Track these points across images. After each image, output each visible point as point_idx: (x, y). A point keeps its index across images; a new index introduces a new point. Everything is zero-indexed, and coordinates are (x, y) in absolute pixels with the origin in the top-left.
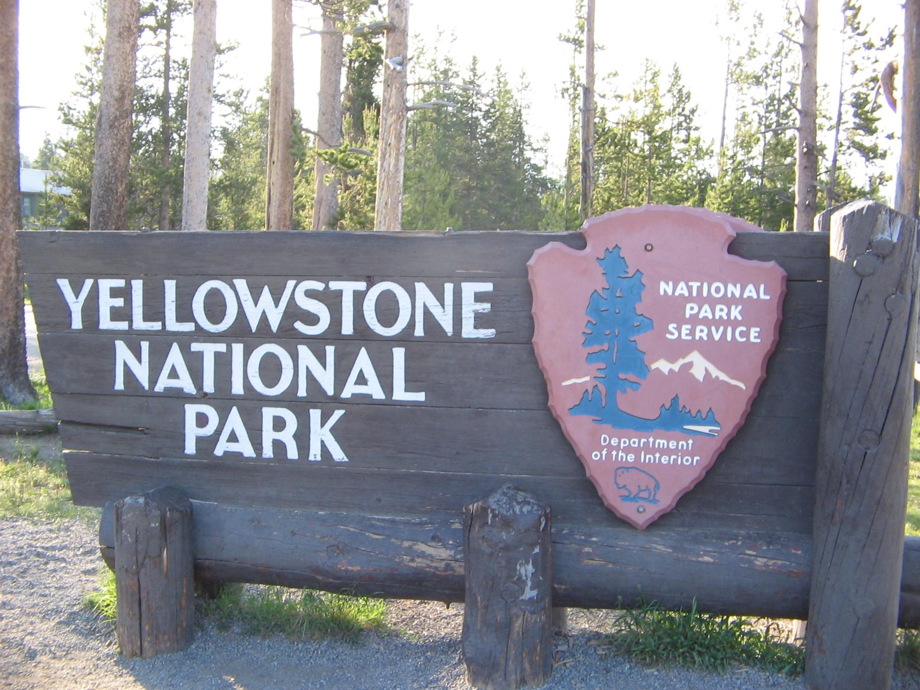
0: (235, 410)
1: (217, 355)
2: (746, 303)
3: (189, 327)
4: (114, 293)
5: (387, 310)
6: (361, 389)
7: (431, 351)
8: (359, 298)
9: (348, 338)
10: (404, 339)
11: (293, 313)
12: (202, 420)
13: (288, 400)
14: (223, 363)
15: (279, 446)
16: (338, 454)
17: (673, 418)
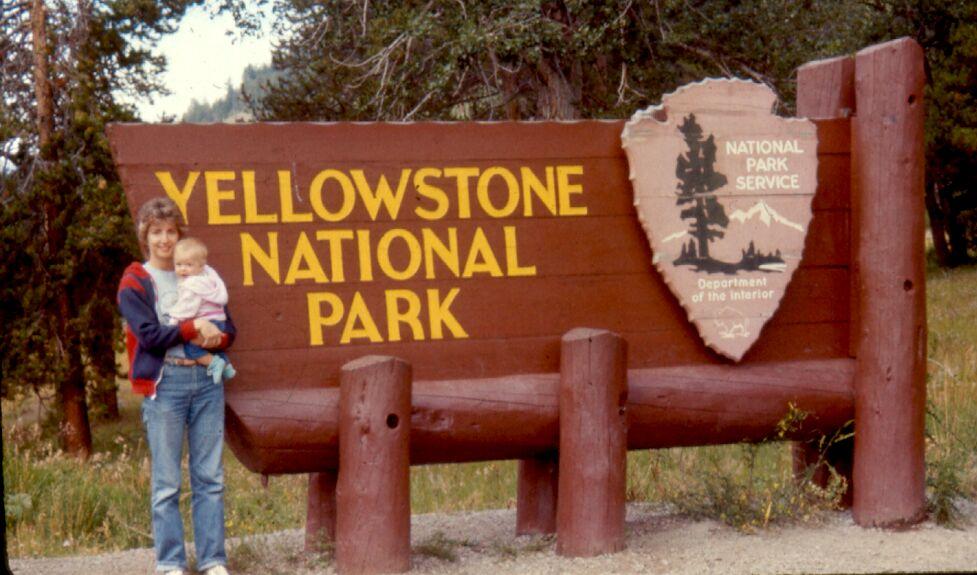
4: (223, 185)
7: (538, 227)
8: (473, 183)
10: (517, 218)
11: (413, 198)
14: (350, 250)
17: (752, 261)
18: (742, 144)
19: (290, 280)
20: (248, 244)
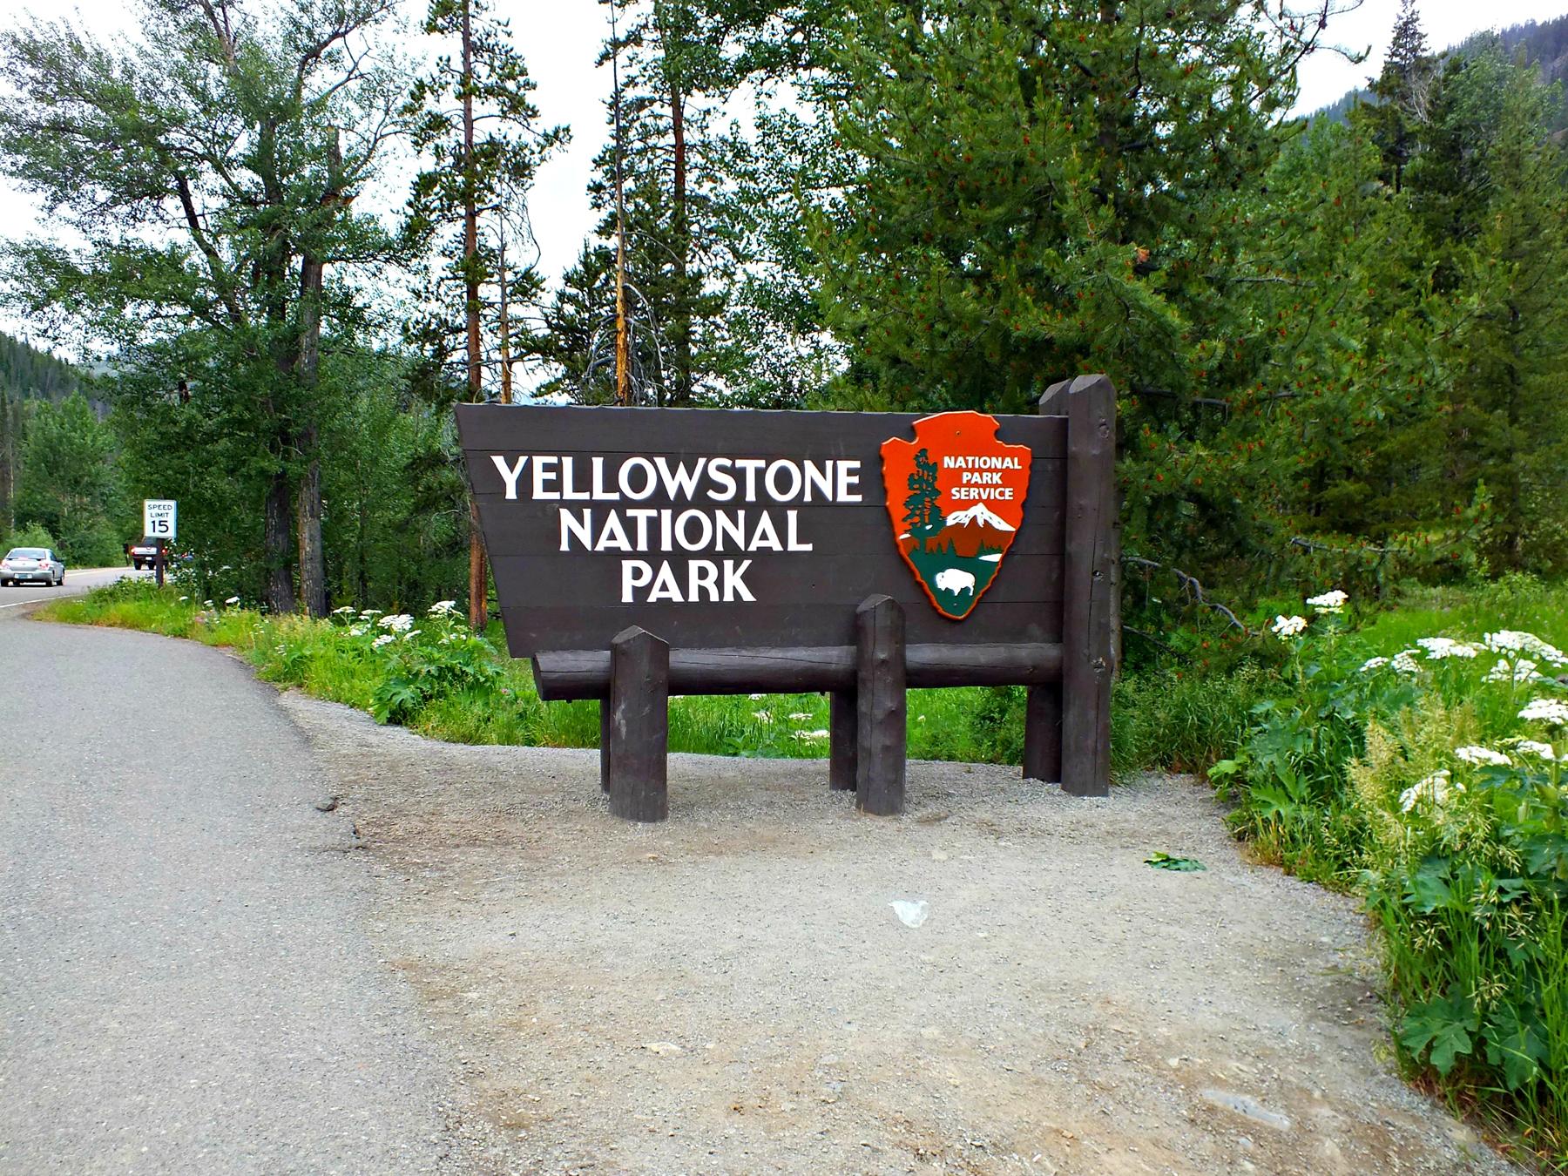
0: (665, 563)
1: (650, 519)
2: (1006, 473)
3: (615, 496)
4: (547, 468)
5: (783, 480)
6: (764, 544)
8: (760, 474)
9: (751, 503)
10: (797, 503)
11: (706, 483)
12: (637, 573)
13: (708, 553)
14: (654, 525)
15: (703, 592)
16: (747, 596)
18: (961, 459)
19: (600, 547)
20: (567, 518)
